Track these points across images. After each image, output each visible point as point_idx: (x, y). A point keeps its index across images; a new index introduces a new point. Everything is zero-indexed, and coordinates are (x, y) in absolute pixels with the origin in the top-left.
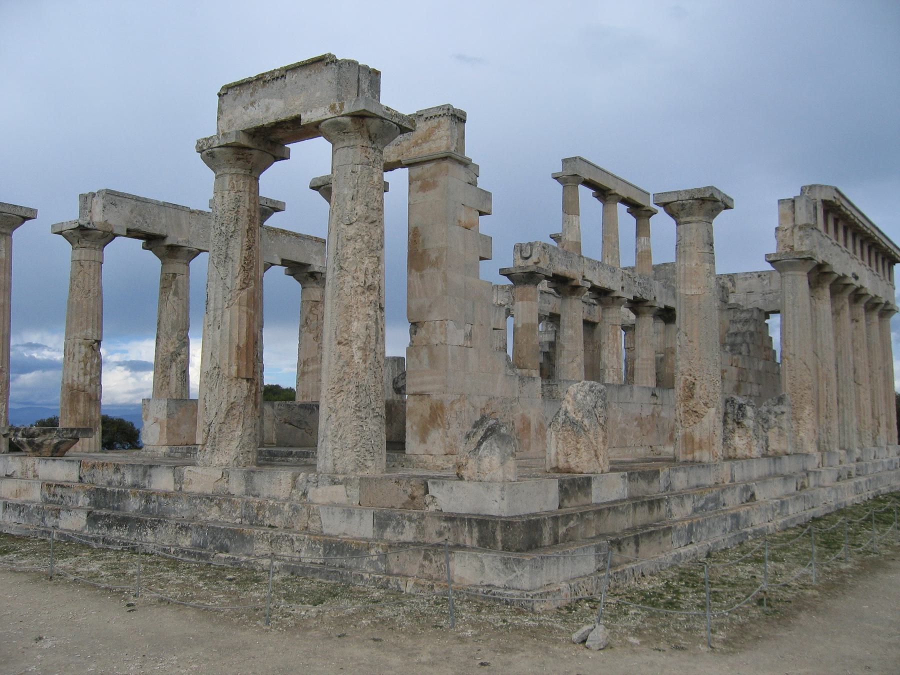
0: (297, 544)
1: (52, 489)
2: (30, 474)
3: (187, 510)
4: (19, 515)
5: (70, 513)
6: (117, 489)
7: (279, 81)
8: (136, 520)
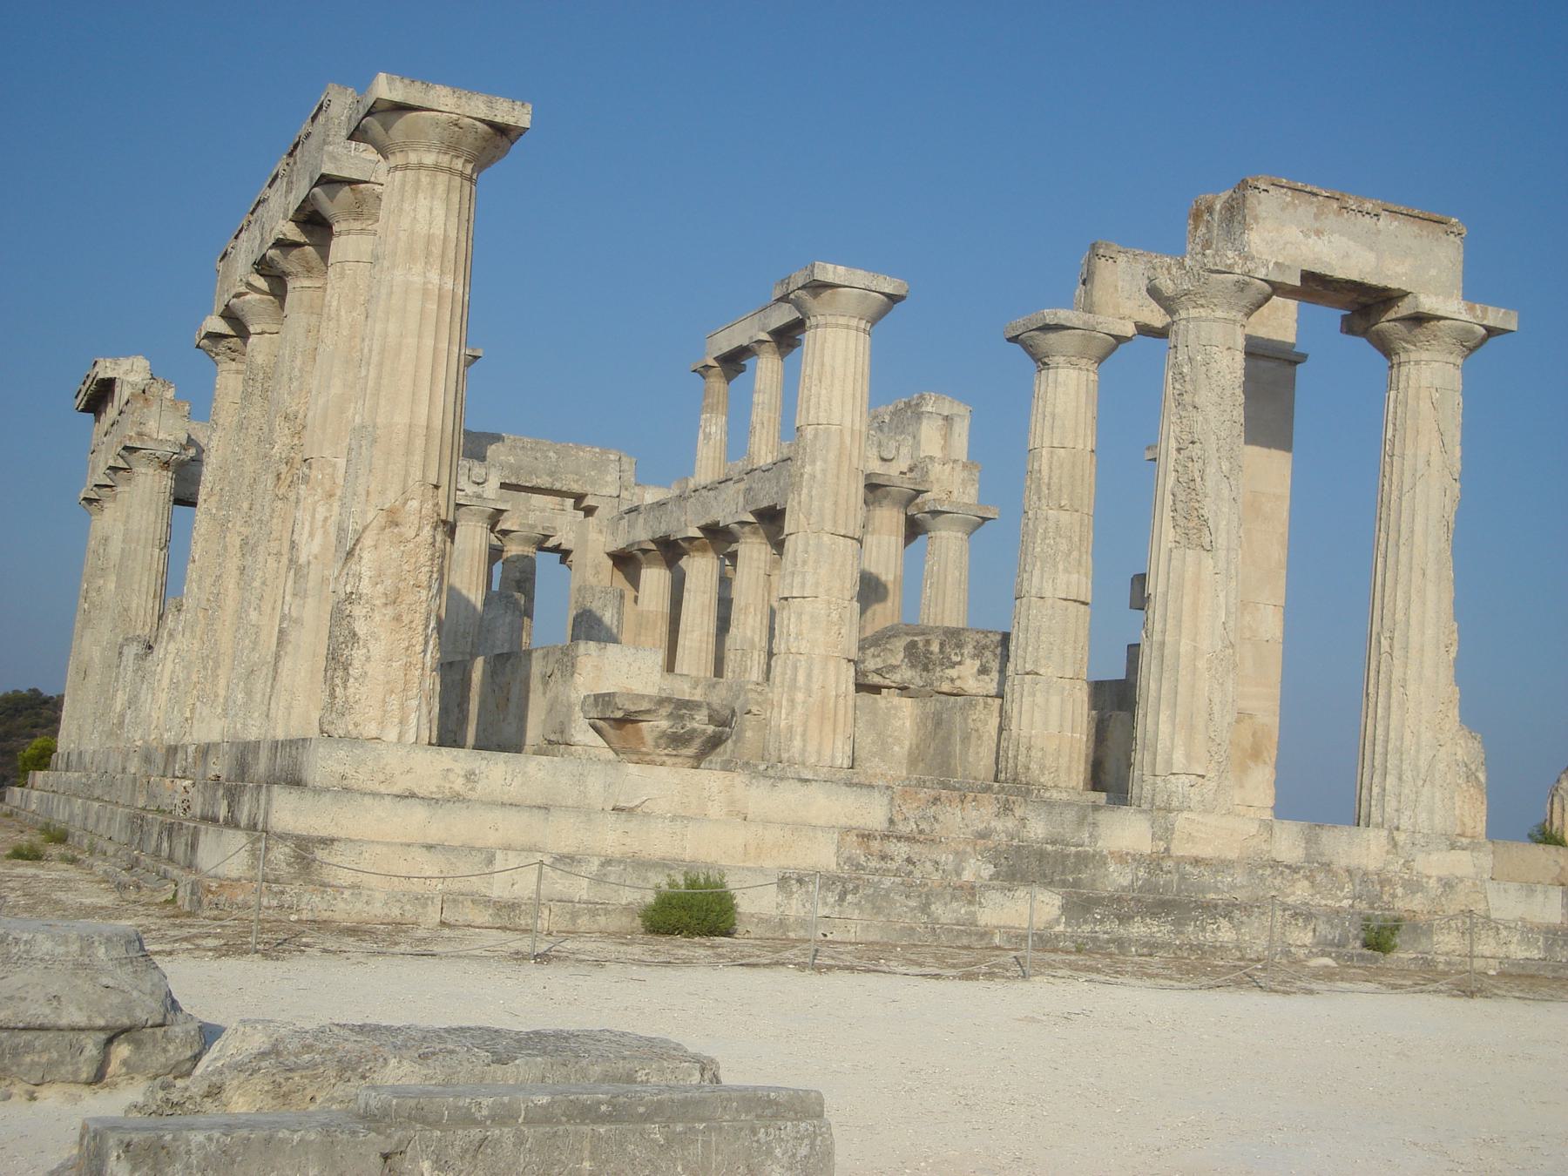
0: (1504, 933)
1: (875, 845)
3: (1243, 887)
4: (842, 898)
5: (1010, 894)
8: (1192, 906)
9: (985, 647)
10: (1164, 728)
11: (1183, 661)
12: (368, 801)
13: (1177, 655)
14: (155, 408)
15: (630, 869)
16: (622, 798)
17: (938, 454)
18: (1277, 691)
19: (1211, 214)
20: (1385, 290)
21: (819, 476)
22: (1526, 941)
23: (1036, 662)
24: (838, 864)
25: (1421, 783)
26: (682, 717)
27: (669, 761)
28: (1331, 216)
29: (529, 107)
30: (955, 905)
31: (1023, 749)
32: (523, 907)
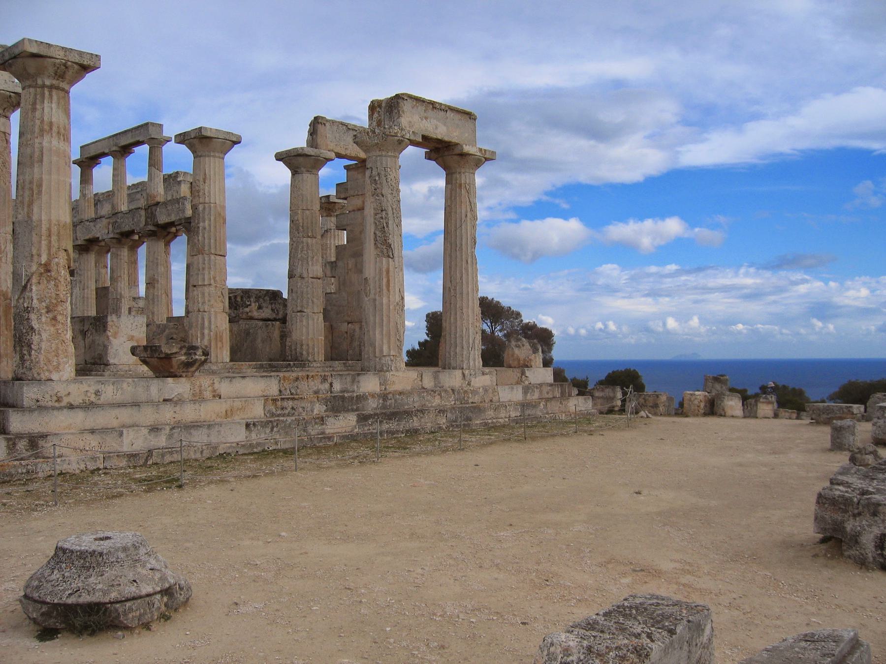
0: (508, 407)
1: (279, 403)
2: (208, 394)
6: (355, 395)
7: (442, 113)
9: (260, 297)
10: (378, 336)
11: (385, 307)
12: (55, 412)
13: (382, 304)
15: (183, 430)
16: (166, 395)
19: (380, 109)
20: (450, 142)
21: (207, 227)
22: (516, 409)
23: (302, 306)
24: (265, 414)
25: (470, 349)
27: (184, 375)
30: (316, 426)
31: (299, 346)
32: (140, 455)
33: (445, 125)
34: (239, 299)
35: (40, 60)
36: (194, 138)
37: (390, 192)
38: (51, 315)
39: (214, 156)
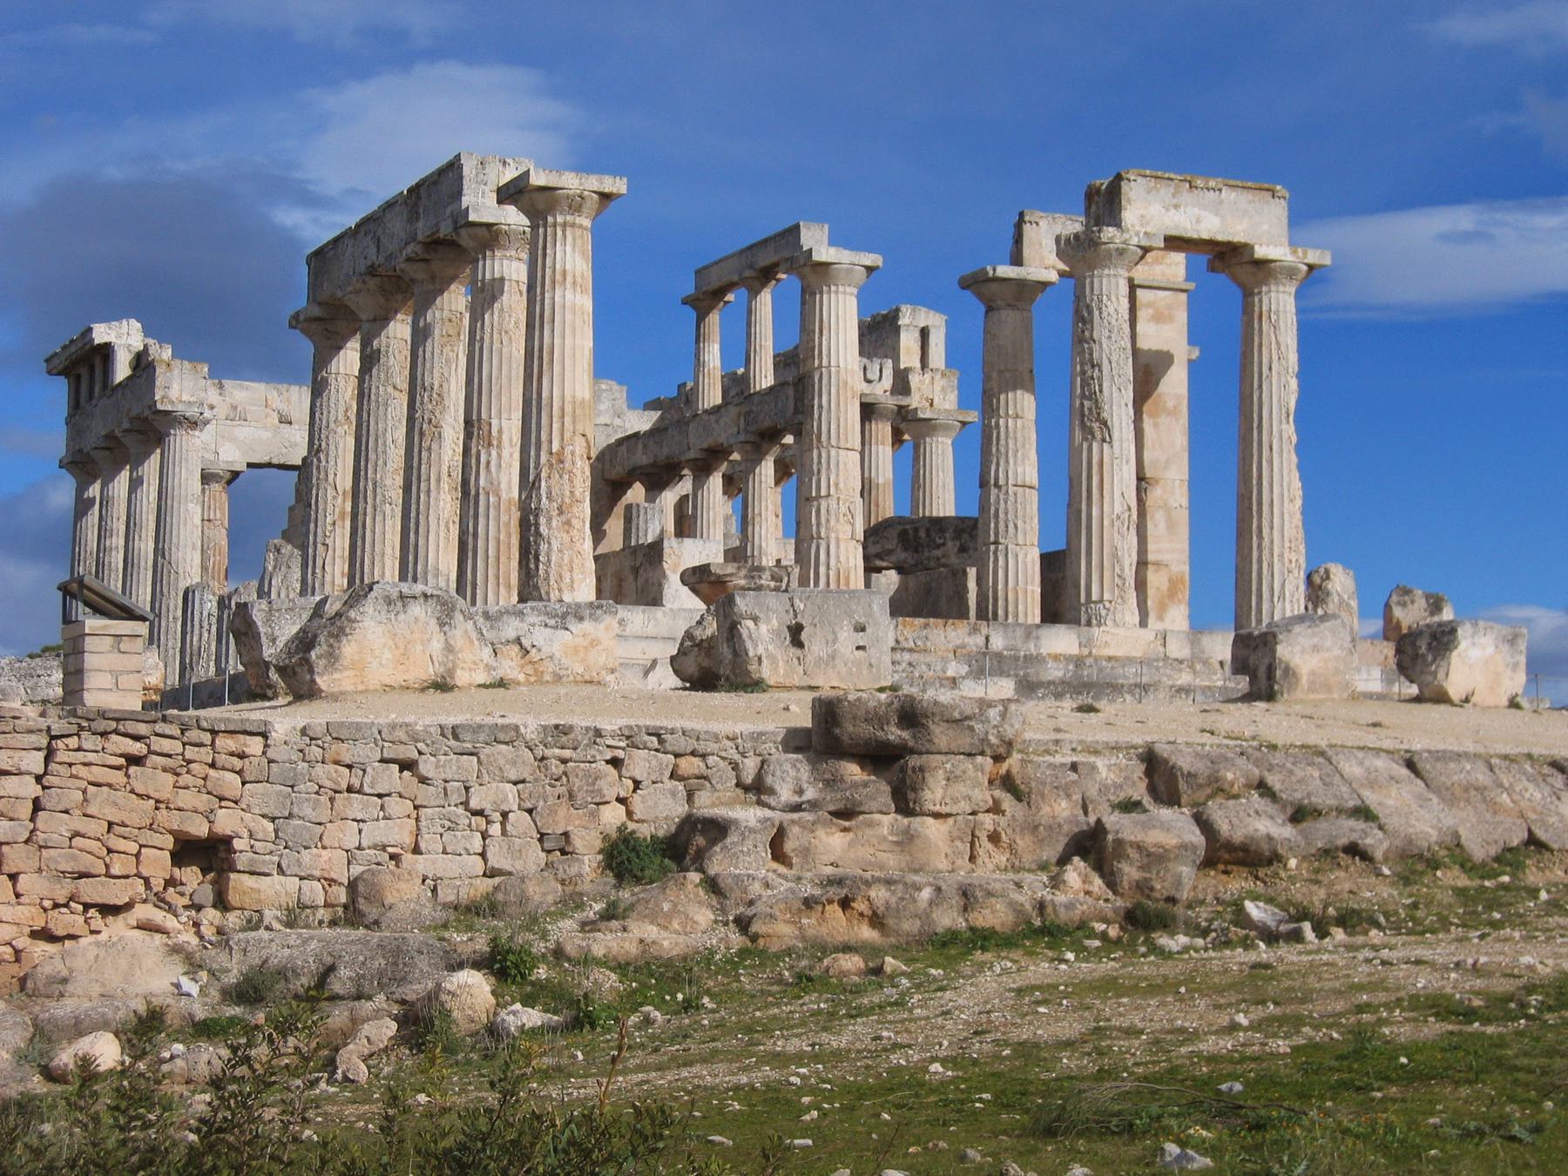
9: (963, 531)
14: (176, 372)
17: (918, 365)
18: (1186, 546)
26: (753, 577)
28: (1185, 193)
29: (625, 180)
33: (1217, 214)
34: (922, 534)
35: (548, 193)
36: (805, 265)
37: (1107, 334)
38: (564, 518)
39: (845, 293)
